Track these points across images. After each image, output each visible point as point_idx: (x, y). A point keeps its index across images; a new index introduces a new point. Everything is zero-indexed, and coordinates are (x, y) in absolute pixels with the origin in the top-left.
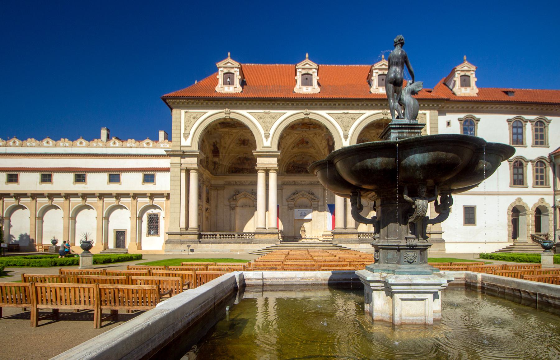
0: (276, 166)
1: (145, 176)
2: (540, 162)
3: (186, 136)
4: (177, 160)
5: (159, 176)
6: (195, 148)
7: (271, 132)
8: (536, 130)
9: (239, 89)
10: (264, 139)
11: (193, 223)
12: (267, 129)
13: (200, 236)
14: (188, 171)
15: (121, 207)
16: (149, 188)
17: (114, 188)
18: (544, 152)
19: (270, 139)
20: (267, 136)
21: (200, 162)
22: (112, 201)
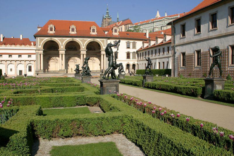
0: (65, 53)
1: (29, 56)
2: (134, 52)
3: (40, 45)
4: (37, 51)
5: (32, 55)
6: (42, 48)
7: (63, 44)
8: (133, 44)
9: (54, 32)
10: (61, 46)
11: (42, 68)
12: (62, 43)
13: (44, 72)
14: (40, 54)
15: (21, 64)
16: (30, 59)
17: (20, 59)
18: (135, 50)
19: (63, 46)
20: (62, 45)
21: (44, 51)
22: (19, 62)
